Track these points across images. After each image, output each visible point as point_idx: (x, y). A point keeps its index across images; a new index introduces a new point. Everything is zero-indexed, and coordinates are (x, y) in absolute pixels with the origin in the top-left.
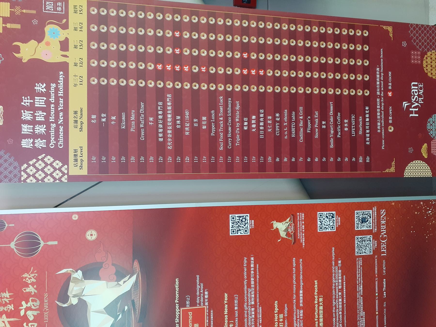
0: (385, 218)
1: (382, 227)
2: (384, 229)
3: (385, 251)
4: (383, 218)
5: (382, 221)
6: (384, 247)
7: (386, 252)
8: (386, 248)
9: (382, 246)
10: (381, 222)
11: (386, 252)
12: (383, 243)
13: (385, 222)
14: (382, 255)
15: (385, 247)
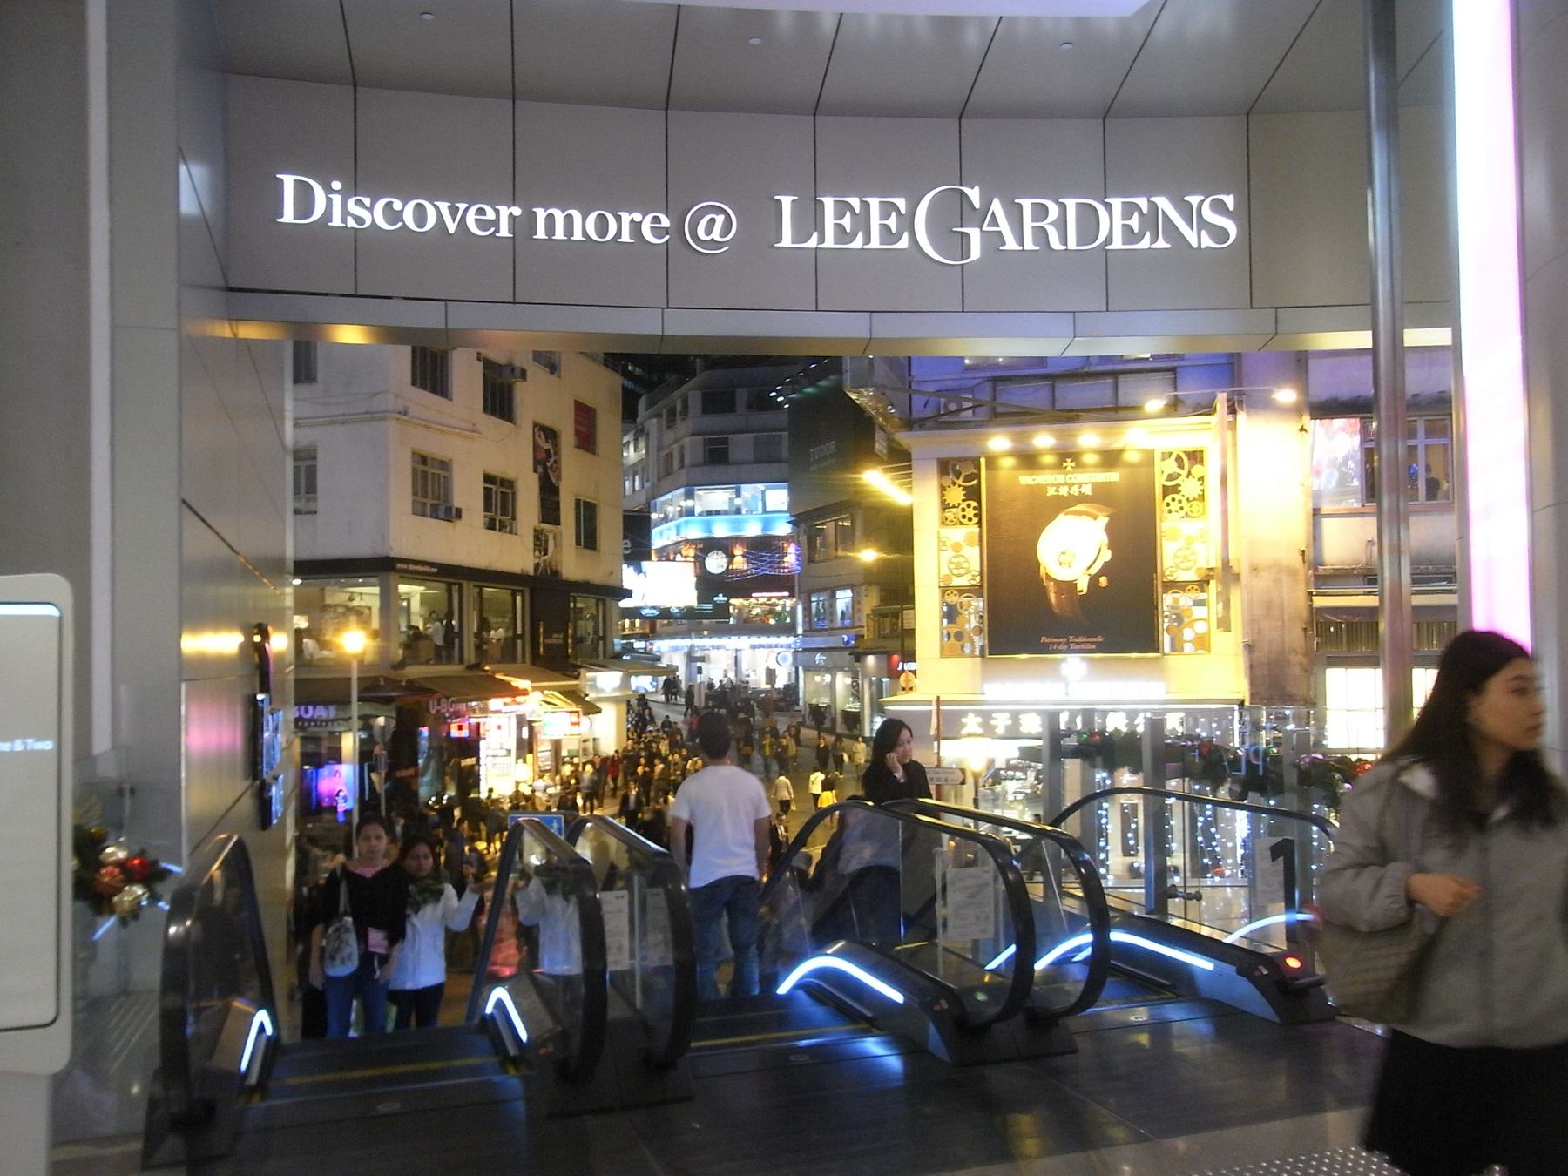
0: (1155, 239)
1: (1063, 207)
2: (1041, 235)
3: (822, 239)
4: (1151, 220)
5: (1129, 210)
6: (862, 221)
7: (812, 243)
8: (858, 243)
9: (874, 203)
10: (1117, 203)
11: (812, 243)
12: (908, 222)
13: (1117, 244)
14: (787, 201)
15: (867, 240)
